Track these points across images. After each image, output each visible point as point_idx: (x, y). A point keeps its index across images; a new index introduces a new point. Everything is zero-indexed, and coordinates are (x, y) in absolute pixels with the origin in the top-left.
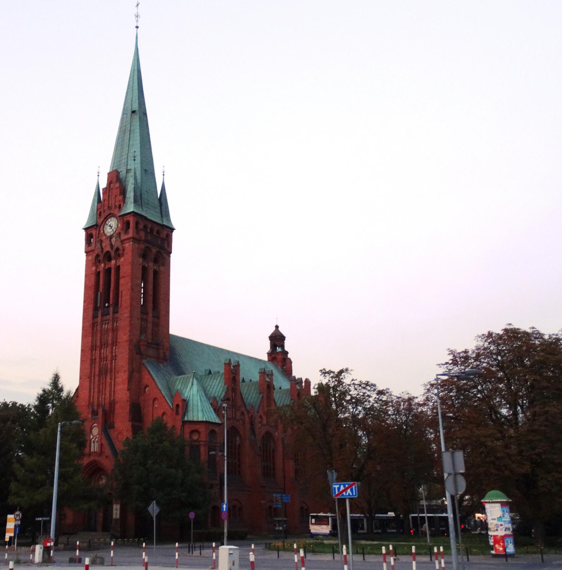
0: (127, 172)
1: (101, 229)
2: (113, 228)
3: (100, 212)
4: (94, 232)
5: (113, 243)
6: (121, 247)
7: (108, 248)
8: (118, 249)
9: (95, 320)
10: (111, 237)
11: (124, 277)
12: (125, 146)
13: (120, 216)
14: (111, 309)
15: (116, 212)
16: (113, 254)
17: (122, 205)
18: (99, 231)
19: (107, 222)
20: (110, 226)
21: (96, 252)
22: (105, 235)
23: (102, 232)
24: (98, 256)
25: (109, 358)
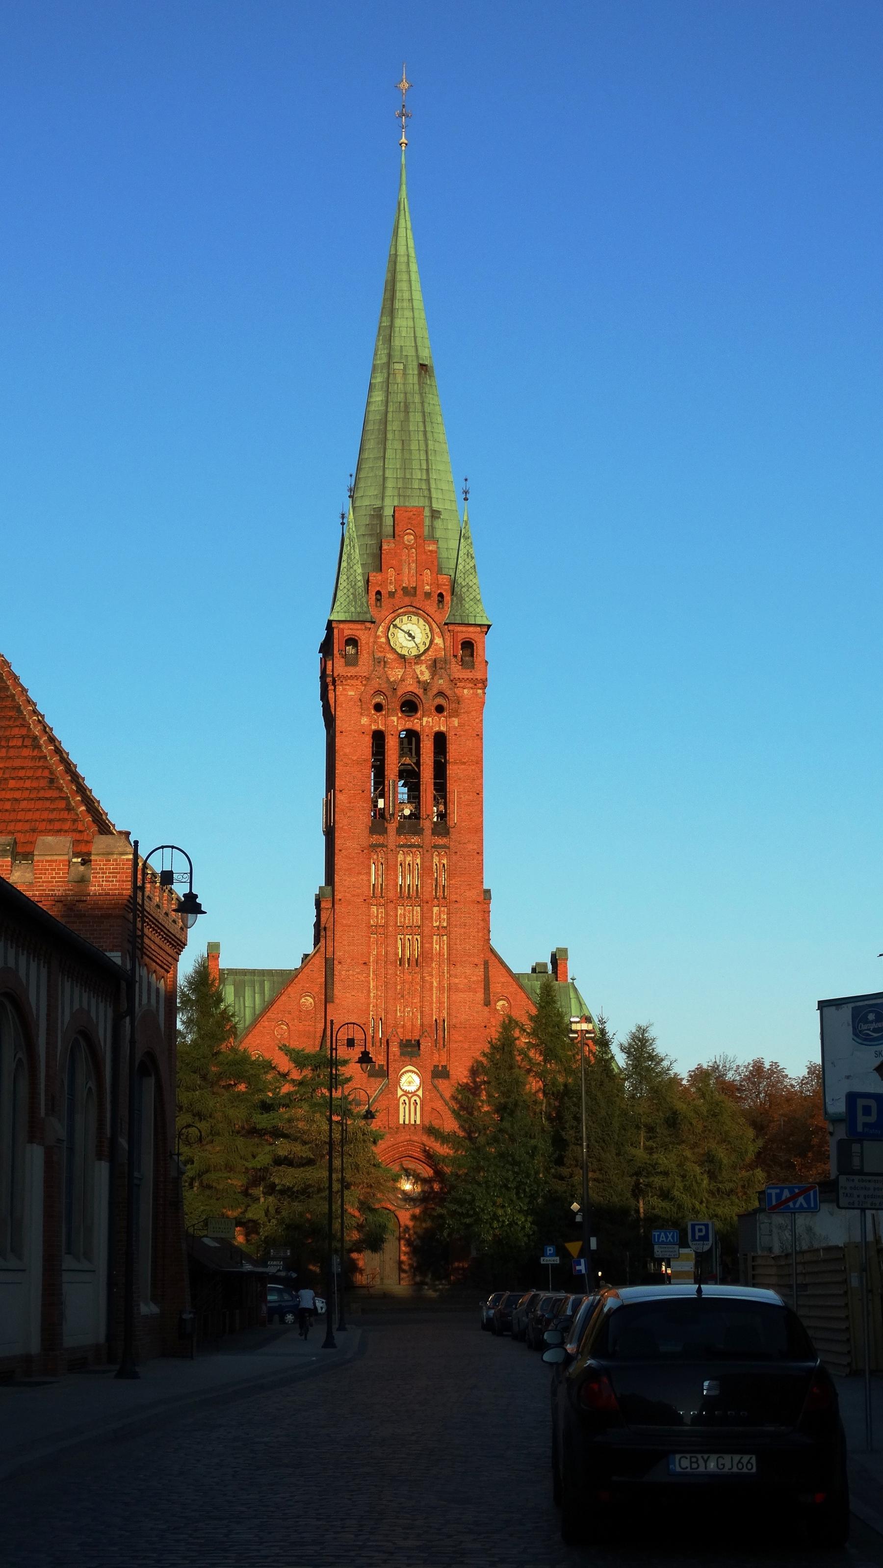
0: (432, 516)
1: (379, 633)
2: (417, 640)
3: (378, 593)
4: (363, 637)
5: (422, 678)
6: (448, 693)
7: (410, 686)
8: (441, 694)
9: (376, 839)
11: (464, 763)
12: (414, 446)
13: (446, 624)
14: (427, 825)
15: (431, 607)
16: (429, 702)
17: (447, 598)
19: (397, 622)
20: (410, 635)
21: (375, 684)
22: (394, 650)
23: (383, 640)
24: (379, 692)
25: (426, 930)
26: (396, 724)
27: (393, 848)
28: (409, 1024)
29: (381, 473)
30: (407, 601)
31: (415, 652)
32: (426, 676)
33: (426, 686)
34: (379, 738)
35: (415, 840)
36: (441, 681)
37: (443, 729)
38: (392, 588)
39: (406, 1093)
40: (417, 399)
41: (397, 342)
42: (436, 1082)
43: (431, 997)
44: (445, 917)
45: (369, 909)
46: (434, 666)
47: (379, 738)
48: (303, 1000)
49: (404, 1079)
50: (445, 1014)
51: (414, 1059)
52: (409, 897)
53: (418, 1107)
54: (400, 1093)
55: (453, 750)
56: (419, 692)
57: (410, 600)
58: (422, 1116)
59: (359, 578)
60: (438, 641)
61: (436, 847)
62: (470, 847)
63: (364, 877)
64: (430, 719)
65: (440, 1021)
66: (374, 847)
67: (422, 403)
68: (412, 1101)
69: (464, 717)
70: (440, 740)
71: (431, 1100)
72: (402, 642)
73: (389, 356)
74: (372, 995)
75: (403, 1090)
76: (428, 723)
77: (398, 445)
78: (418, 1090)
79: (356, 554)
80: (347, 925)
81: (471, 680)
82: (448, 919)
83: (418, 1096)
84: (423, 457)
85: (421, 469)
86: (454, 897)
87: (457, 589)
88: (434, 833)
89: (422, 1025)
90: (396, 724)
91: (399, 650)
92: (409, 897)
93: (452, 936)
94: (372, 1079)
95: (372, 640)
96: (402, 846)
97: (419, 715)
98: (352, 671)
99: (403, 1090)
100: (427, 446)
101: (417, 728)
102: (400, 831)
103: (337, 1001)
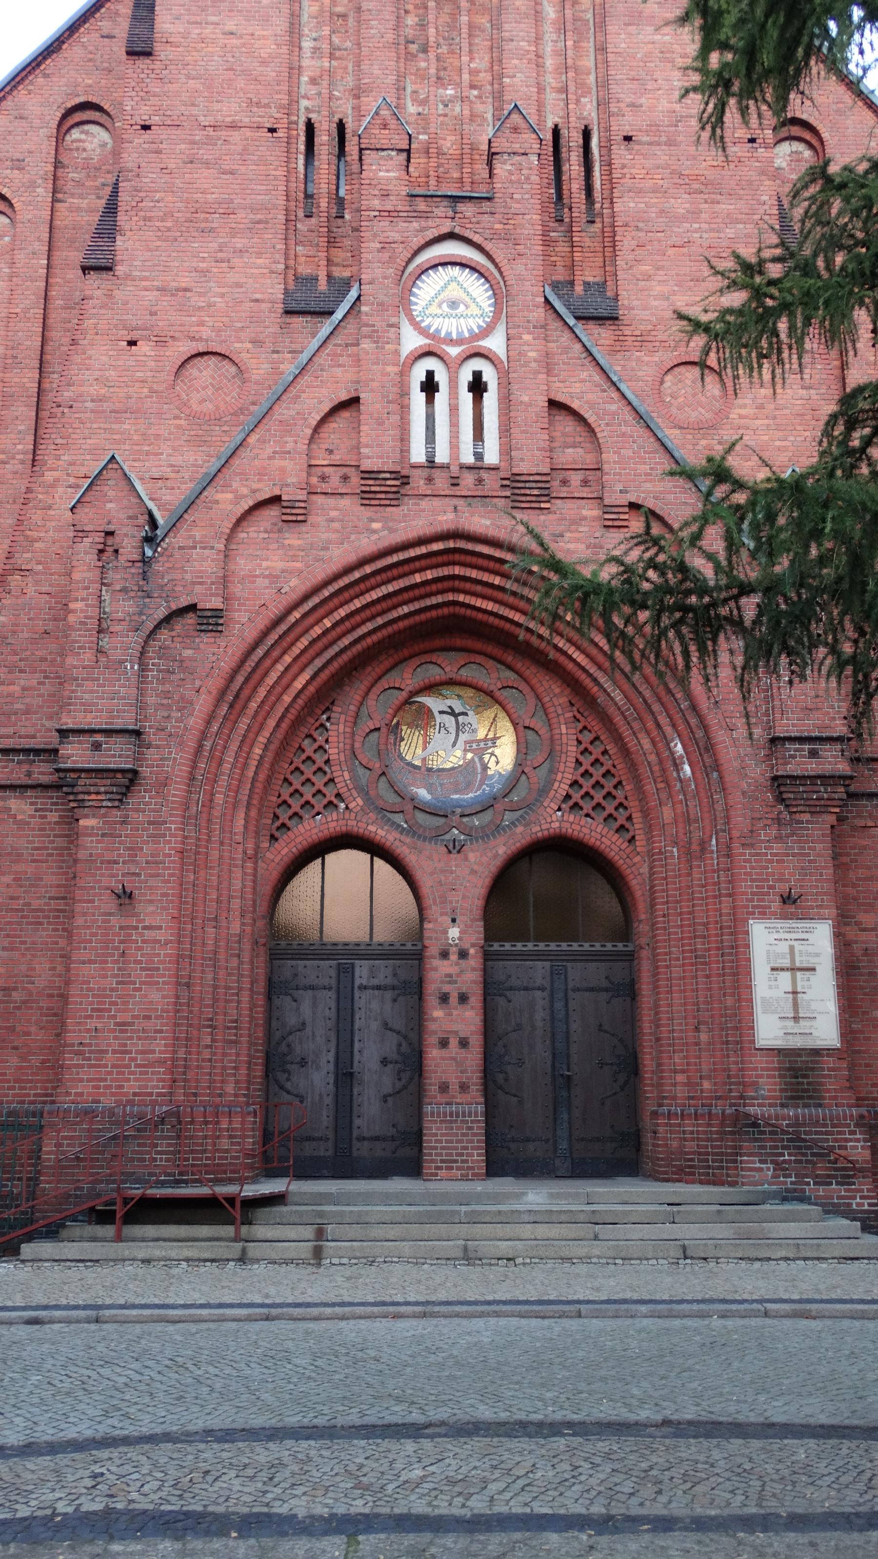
28: (449, 144)
43: (538, 39)
48: (75, 134)
49: (429, 290)
50: (589, 109)
58: (505, 430)
65: (573, 139)
68: (465, 376)
71: (548, 366)
74: (307, 44)
78: (486, 332)
99: (423, 332)
103: (162, 52)
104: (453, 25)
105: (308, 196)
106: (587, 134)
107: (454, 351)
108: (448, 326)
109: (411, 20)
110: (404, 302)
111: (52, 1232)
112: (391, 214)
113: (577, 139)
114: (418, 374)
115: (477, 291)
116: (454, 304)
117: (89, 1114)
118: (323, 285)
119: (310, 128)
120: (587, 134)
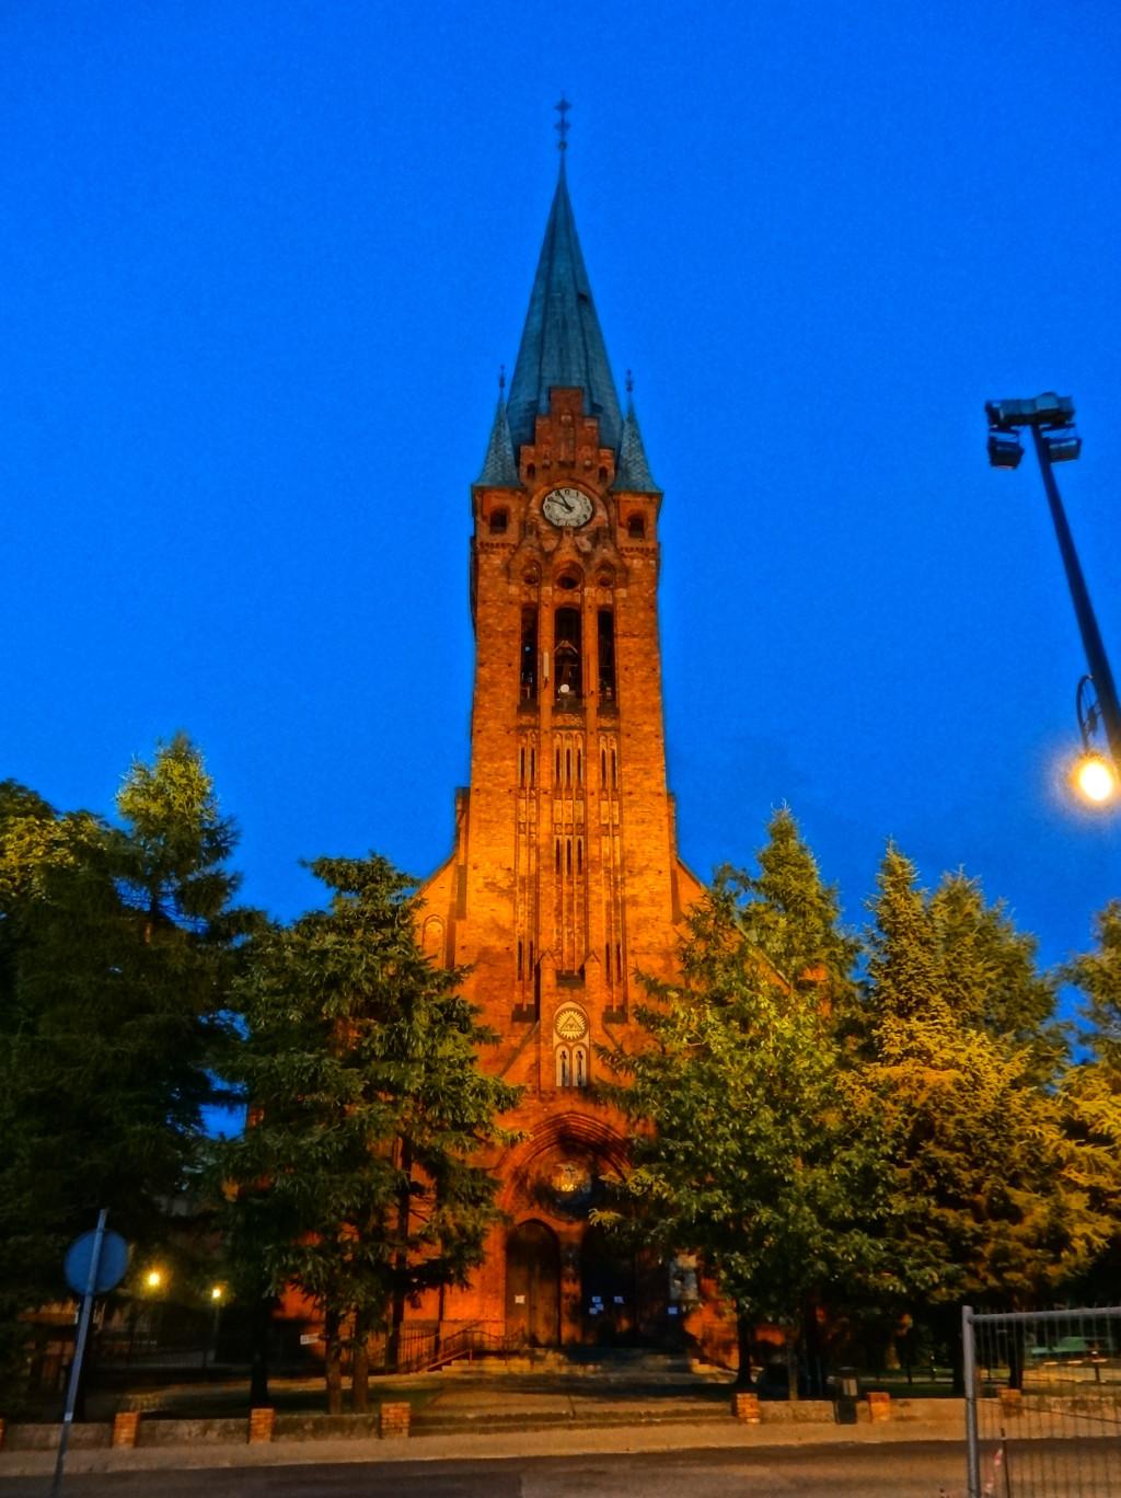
3: (531, 469)
4: (513, 505)
6: (615, 562)
7: (566, 555)
8: (606, 565)
9: (525, 719)
10: (577, 530)
11: (634, 636)
14: (591, 703)
18: (528, 509)
22: (549, 522)
23: (537, 512)
26: (551, 595)
27: (548, 729)
29: (536, 373)
30: (565, 473)
31: (574, 524)
32: (587, 547)
33: (587, 556)
34: (530, 614)
35: (576, 721)
36: (605, 551)
37: (610, 602)
38: (547, 462)
39: (565, 1040)
40: (575, 317)
41: (555, 279)
42: (608, 1026)
44: (617, 813)
45: (517, 804)
46: (596, 538)
47: (530, 614)
51: (576, 992)
52: (569, 788)
53: (584, 1062)
54: (556, 1040)
55: (620, 625)
56: (579, 560)
57: (568, 474)
59: (508, 452)
60: (601, 513)
61: (601, 729)
62: (647, 728)
63: (509, 763)
64: (593, 590)
66: (521, 729)
67: (581, 321)
68: (575, 1053)
69: (634, 589)
70: (606, 619)
72: (557, 512)
73: (548, 290)
75: (561, 1037)
76: (591, 596)
77: (555, 352)
78: (582, 1036)
79: (507, 432)
80: (485, 821)
81: (641, 550)
82: (621, 815)
83: (583, 1045)
84: (582, 361)
85: (581, 371)
86: (627, 788)
87: (623, 465)
88: (600, 712)
89: (587, 950)
90: (551, 596)
91: (555, 523)
92: (569, 788)
93: (626, 835)
94: (517, 1024)
95: (523, 510)
96: (560, 728)
97: (579, 587)
98: (498, 539)
99: (561, 1037)
100: (586, 351)
101: (578, 600)
102: (556, 710)
103: (469, 917)
104: (571, 903)
105: (520, 968)
106: (618, 947)
107: (571, 1044)
108: (570, 1034)
109: (555, 901)
110: (553, 1025)
111: (449, 1363)
112: (548, 994)
113: (614, 949)
114: (559, 1052)
115: (579, 1019)
116: (571, 1026)
117: (455, 1322)
118: (525, 1009)
119: (520, 945)
120: (618, 947)
